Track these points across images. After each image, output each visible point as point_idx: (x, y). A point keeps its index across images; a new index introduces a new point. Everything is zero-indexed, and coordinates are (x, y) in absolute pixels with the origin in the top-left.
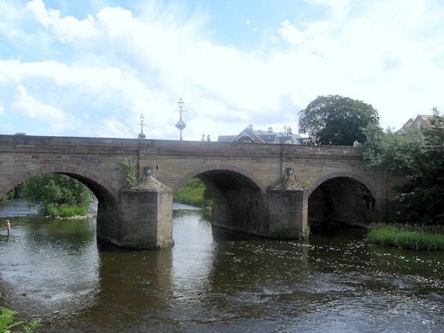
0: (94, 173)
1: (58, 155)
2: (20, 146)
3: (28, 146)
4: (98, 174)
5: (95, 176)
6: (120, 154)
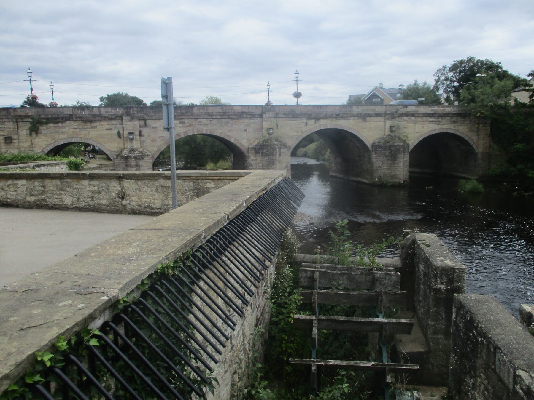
0: (228, 133)
1: (199, 120)
5: (228, 136)
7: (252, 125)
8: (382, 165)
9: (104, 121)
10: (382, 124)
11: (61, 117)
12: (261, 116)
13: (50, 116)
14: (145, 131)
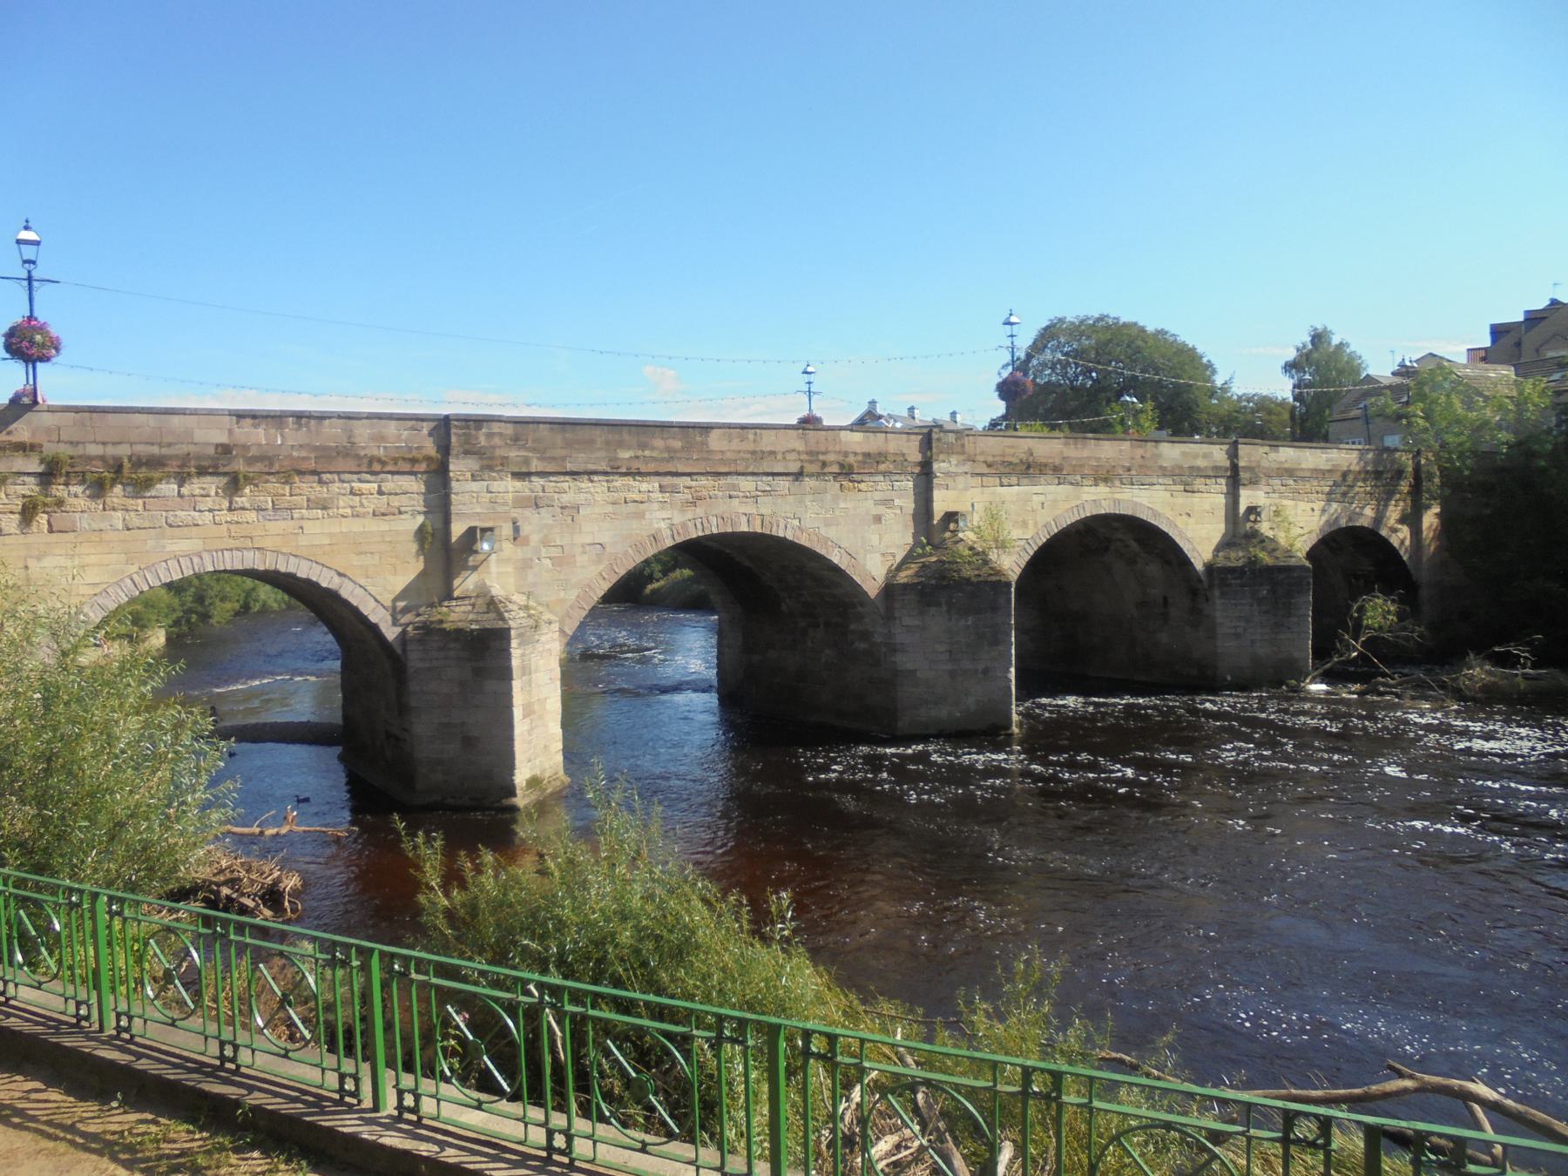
0: (823, 531)
1: (730, 480)
2: (625, 454)
3: (647, 453)
4: (831, 533)
6: (884, 474)
7: (897, 502)
8: (1245, 629)
9: (368, 477)
11: (177, 456)
13: (123, 451)
14: (532, 523)
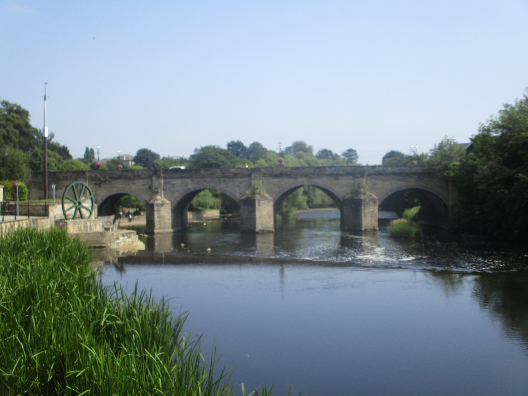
10: (352, 181)
12: (250, 175)
